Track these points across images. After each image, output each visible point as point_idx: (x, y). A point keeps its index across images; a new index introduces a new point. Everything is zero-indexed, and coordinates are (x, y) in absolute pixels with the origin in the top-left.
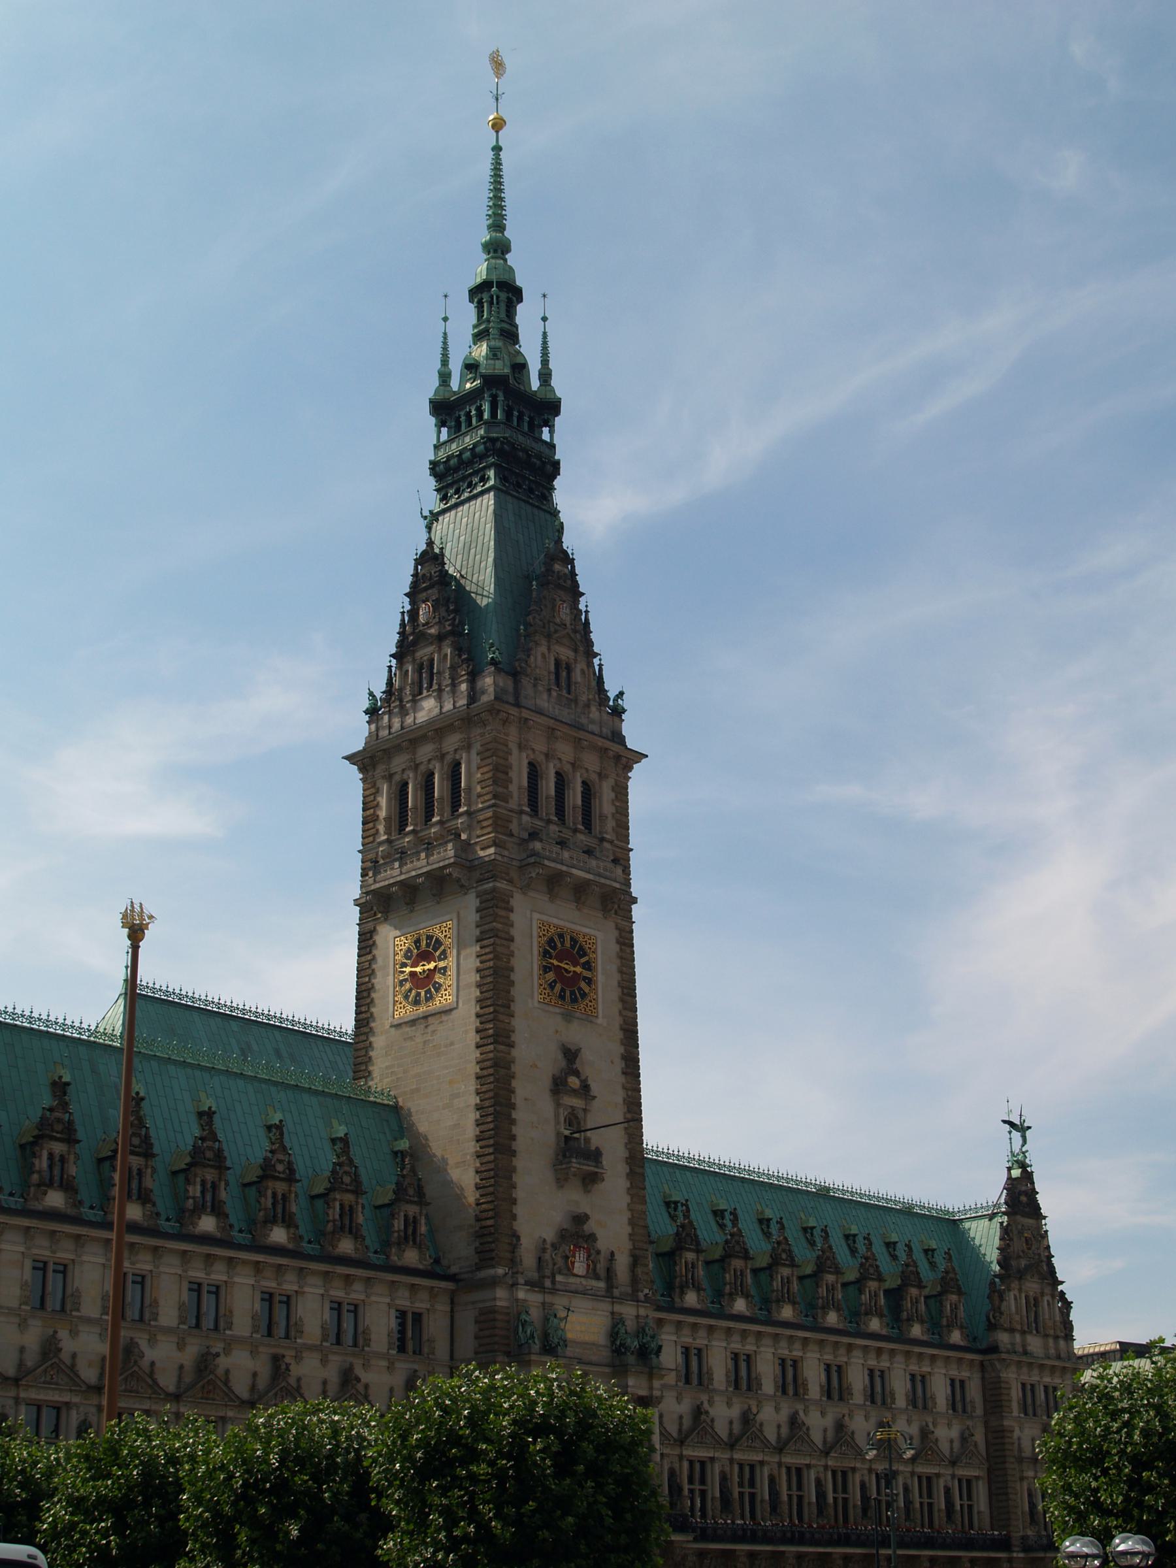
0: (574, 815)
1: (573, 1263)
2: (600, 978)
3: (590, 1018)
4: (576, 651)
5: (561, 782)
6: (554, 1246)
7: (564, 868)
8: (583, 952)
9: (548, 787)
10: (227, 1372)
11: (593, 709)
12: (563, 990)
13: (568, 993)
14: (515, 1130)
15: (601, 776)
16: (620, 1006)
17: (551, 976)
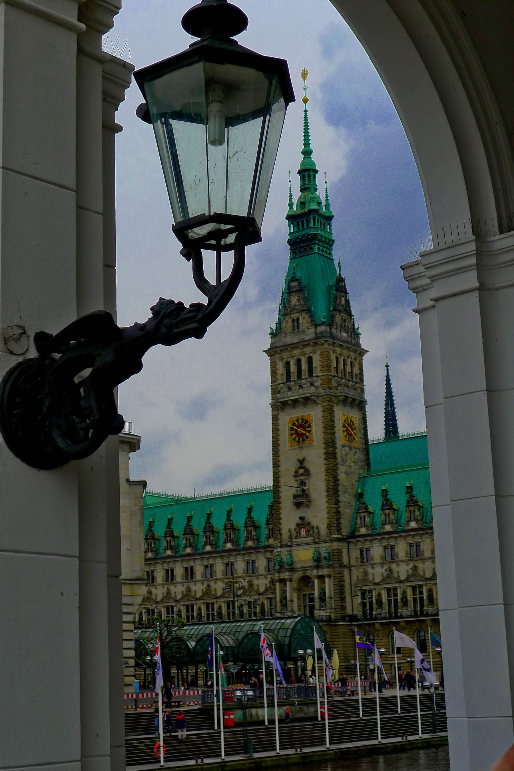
0: (305, 374)
1: (300, 534)
2: (314, 428)
3: (310, 445)
4: (298, 312)
5: (299, 362)
6: (295, 529)
7: (287, 399)
8: (307, 422)
9: (293, 368)
10: (216, 589)
11: (306, 330)
12: (299, 439)
13: (301, 439)
14: (280, 495)
15: (315, 352)
16: (324, 435)
17: (294, 436)
